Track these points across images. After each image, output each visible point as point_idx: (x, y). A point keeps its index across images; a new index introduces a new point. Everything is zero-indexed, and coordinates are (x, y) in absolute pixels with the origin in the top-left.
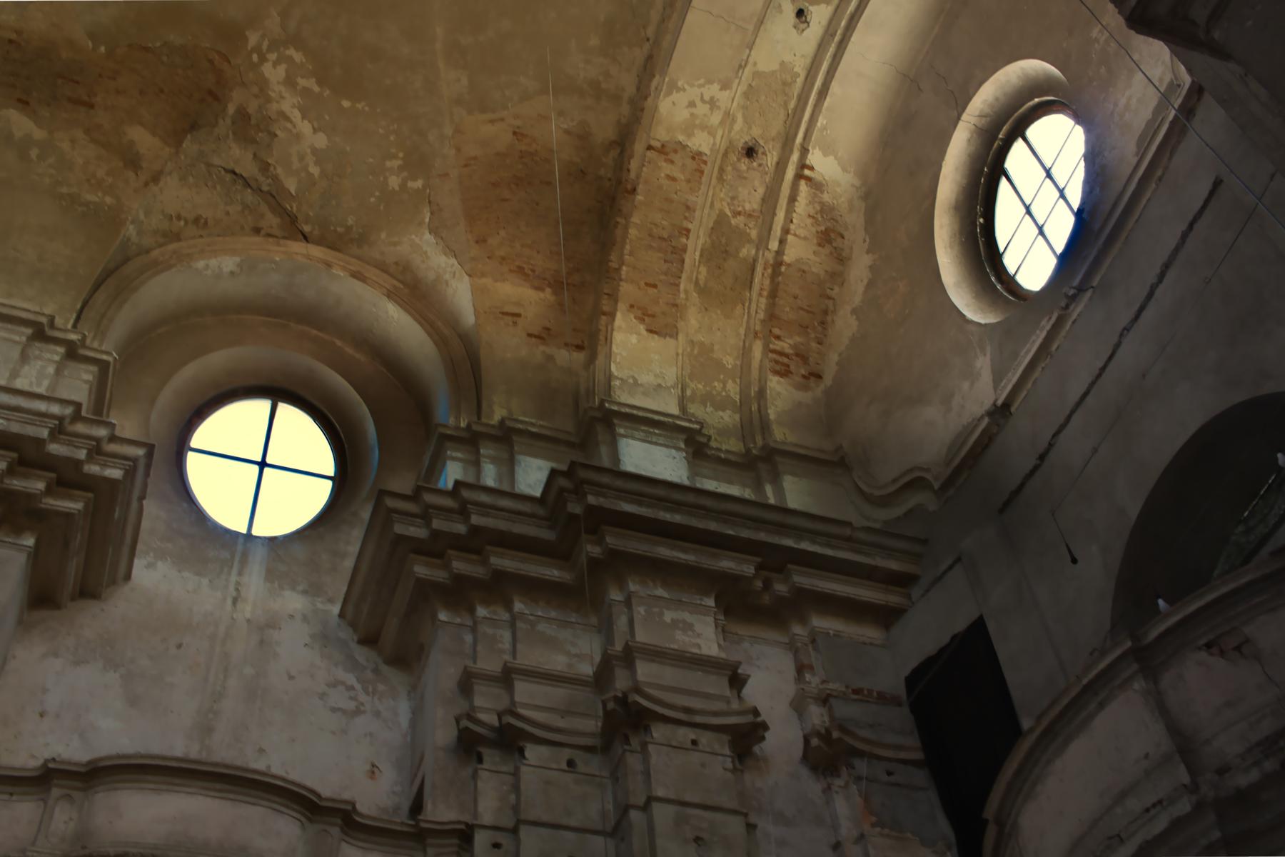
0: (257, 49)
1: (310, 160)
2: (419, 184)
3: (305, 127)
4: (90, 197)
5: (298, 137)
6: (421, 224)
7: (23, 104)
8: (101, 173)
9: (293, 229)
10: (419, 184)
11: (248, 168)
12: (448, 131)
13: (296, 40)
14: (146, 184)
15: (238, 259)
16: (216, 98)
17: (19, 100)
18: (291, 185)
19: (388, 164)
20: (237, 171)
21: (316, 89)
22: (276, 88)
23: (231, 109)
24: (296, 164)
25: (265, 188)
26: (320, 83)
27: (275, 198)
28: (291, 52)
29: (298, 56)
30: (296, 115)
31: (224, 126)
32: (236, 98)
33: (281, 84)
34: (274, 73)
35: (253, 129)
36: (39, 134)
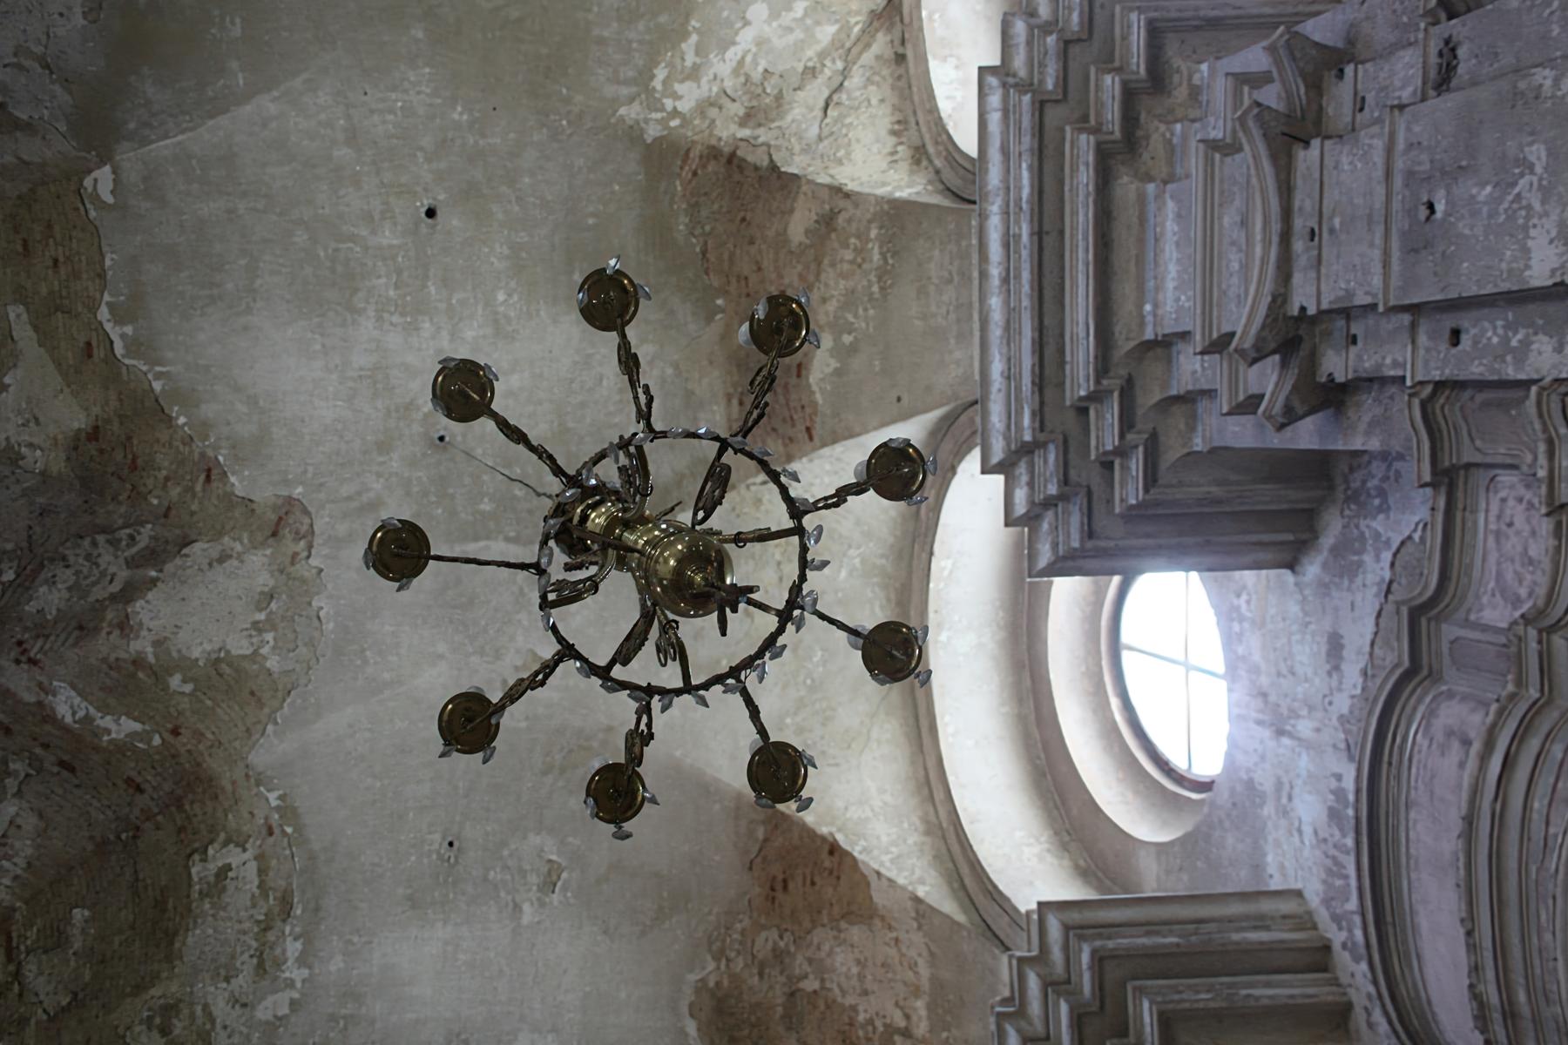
4: (876, 257)
17: (799, 376)
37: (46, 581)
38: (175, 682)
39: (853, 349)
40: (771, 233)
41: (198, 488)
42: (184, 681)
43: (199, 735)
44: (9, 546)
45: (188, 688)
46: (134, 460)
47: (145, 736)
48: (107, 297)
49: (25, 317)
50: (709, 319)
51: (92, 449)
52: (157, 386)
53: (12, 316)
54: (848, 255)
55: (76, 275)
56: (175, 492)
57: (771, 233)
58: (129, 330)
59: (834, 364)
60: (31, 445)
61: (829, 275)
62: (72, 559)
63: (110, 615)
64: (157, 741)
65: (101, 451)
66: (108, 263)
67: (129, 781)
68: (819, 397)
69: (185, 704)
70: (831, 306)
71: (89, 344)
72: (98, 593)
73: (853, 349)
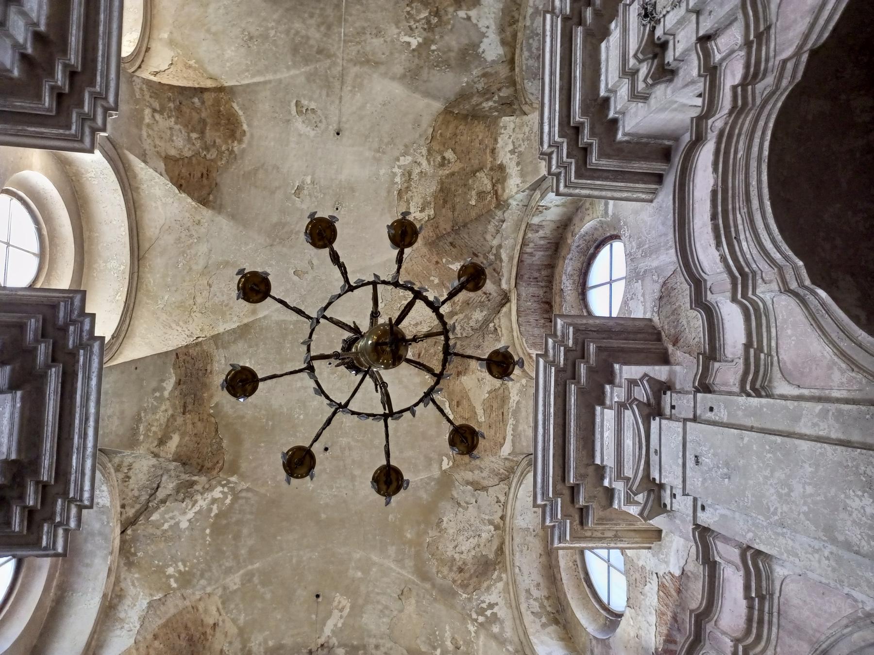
0: (229, 482)
1: (172, 522)
2: (174, 585)
3: (190, 515)
4: (141, 428)
5: (185, 513)
6: (151, 595)
7: (179, 383)
8: (154, 429)
9: (127, 524)
10: (174, 585)
11: (161, 494)
12: (209, 590)
13: (236, 498)
14: (152, 453)
15: (108, 504)
16: (200, 470)
17: (180, 380)
18: (155, 517)
19: (180, 564)
20: (159, 489)
21: (212, 515)
22: (209, 496)
23: (195, 478)
24: (167, 516)
25: (150, 505)
26: (216, 515)
27: (146, 510)
28: (230, 497)
29: (228, 501)
30: (197, 508)
31: (185, 477)
32: (202, 479)
33: (212, 497)
34: (217, 493)
35: (186, 491)
36: (166, 394)
38: (436, 281)
39: (155, 390)
40: (187, 438)
41: (423, 352)
42: (433, 281)
43: (429, 261)
45: (432, 278)
47: (448, 262)
50: (217, 405)
54: (154, 429)
56: (432, 351)
57: (187, 438)
59: (164, 385)
61: (163, 420)
63: (458, 308)
64: (444, 260)
67: (454, 247)
68: (172, 371)
69: (433, 272)
70: (163, 408)
72: (461, 316)
73: (155, 390)
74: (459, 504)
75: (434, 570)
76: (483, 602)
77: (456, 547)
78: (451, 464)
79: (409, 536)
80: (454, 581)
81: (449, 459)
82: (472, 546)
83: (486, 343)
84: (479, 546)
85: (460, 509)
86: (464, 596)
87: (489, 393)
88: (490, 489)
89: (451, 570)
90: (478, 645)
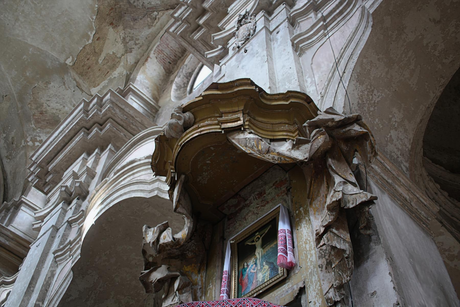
37: (150, 4)
44: (149, 19)
46: (111, 10)
48: (87, 43)
49: (100, 59)
51: (114, 22)
52: (94, 17)
53: (101, 61)
55: (87, 53)
58: (89, 33)
60: (120, 37)
62: (141, 3)
65: (114, 19)
66: (81, 48)
71: (97, 40)
74: (64, 84)
75: (29, 102)
76: (40, 137)
77: (48, 101)
78: (71, 64)
79: (28, 74)
80: (34, 115)
81: (73, 60)
82: (57, 108)
83: (141, 22)
84: (60, 111)
85: (63, 86)
86: (33, 126)
87: (113, 53)
88: (84, 93)
89: (37, 108)
90: (20, 152)
